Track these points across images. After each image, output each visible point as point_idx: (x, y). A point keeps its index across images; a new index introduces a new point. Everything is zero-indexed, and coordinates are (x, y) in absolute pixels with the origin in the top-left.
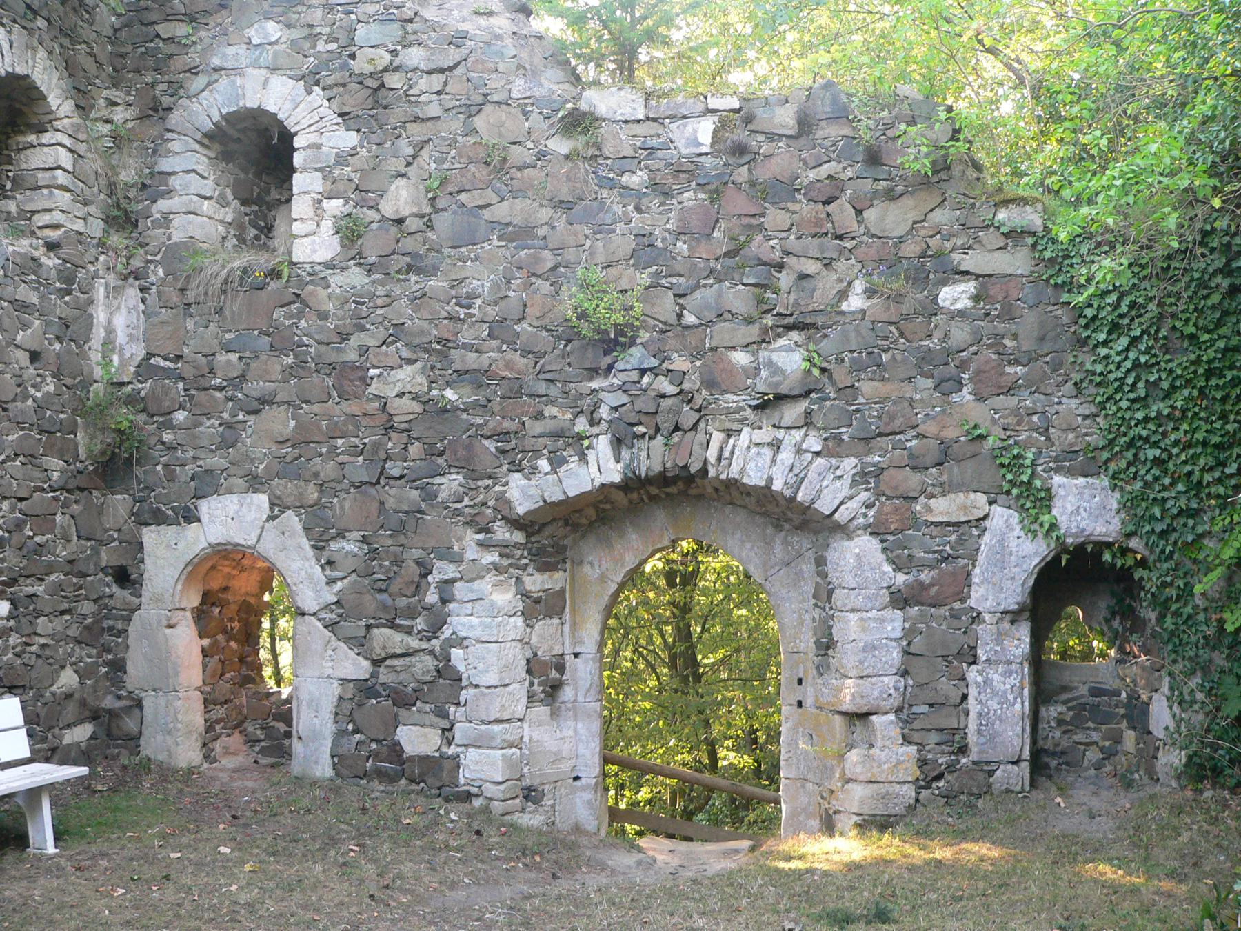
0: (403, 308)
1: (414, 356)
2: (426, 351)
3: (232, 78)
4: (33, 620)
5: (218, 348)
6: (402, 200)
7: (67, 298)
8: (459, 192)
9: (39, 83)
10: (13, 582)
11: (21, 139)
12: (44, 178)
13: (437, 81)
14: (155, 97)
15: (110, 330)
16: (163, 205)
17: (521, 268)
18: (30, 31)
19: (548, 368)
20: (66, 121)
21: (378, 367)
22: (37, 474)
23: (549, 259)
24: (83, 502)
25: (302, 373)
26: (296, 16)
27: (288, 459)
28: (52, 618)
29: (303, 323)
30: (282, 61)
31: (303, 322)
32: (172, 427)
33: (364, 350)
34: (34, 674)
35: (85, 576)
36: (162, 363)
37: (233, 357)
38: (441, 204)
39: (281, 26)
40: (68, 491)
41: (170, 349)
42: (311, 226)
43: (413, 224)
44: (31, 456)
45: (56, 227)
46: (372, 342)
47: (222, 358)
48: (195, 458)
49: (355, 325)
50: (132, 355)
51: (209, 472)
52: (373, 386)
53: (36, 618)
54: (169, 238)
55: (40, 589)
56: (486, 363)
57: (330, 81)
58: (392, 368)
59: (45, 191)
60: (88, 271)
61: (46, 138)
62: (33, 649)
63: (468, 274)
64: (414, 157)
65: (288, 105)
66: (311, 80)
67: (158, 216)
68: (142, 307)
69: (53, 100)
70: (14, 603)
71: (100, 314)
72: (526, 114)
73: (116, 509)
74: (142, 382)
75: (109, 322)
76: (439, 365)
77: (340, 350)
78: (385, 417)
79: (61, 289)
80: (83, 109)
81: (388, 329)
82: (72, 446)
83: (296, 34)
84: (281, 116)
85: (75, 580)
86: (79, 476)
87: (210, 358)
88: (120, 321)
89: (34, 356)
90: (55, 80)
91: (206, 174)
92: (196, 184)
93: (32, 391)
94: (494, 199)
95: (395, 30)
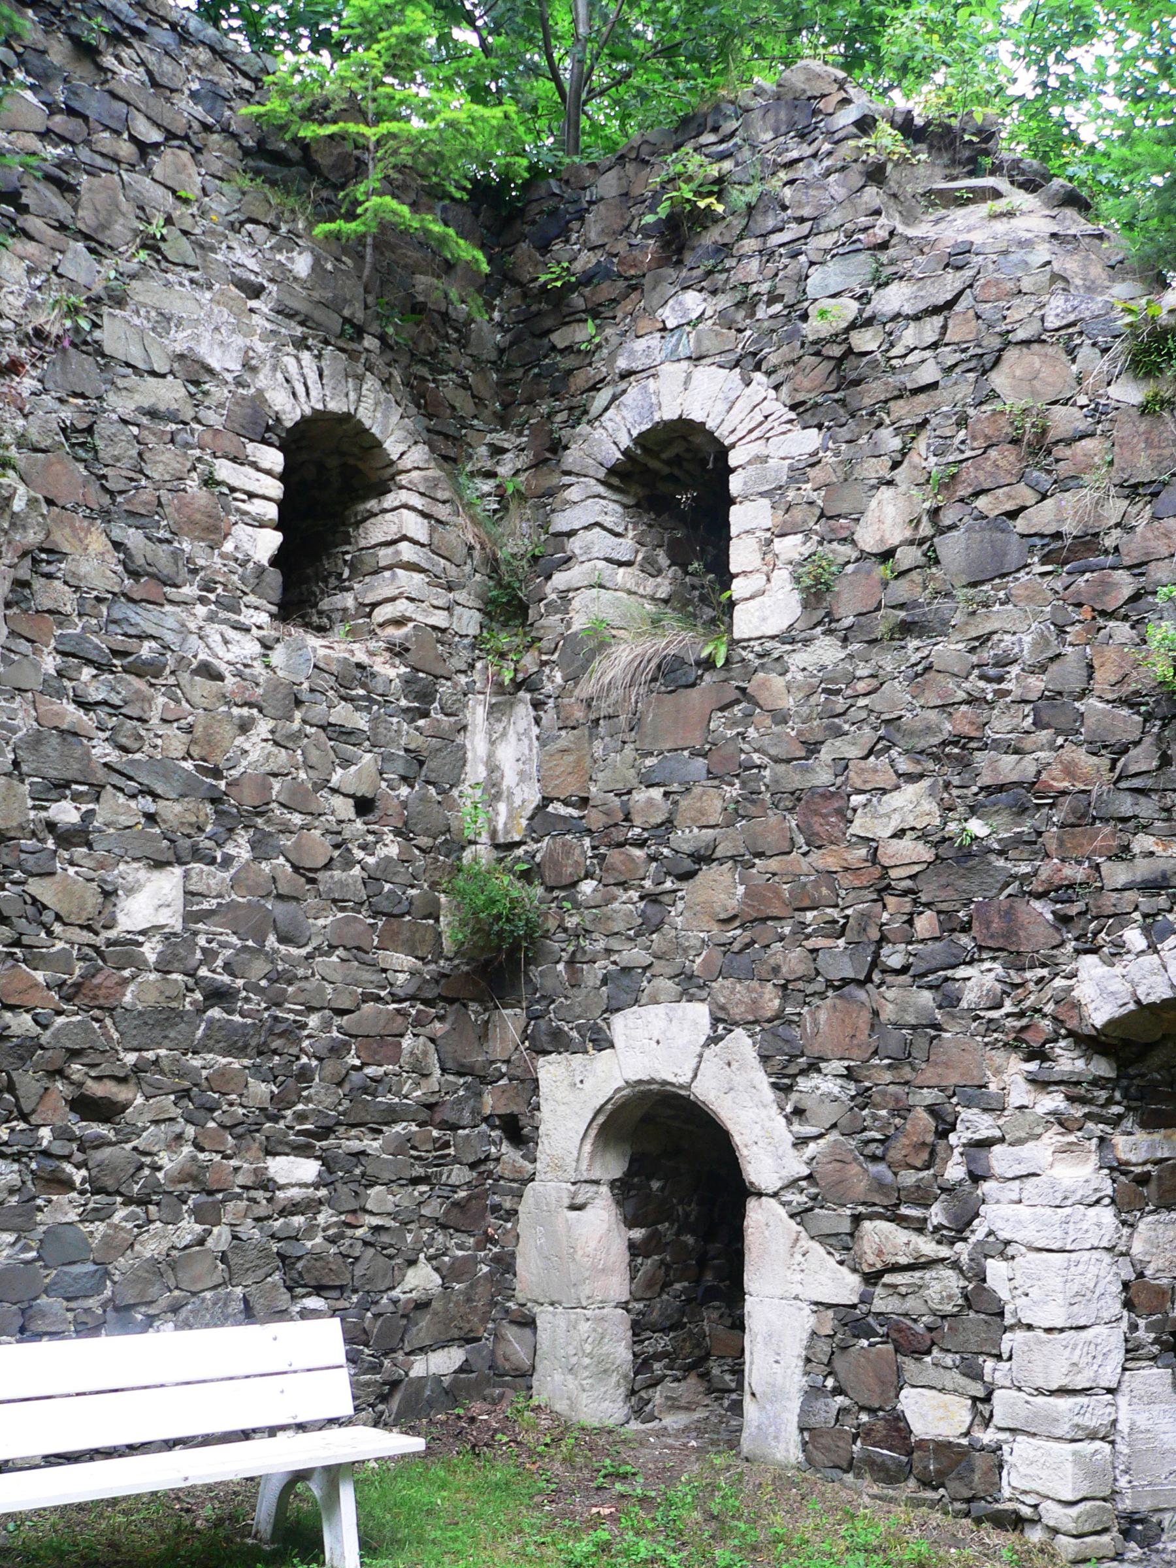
0: (897, 694)
1: (918, 769)
2: (936, 758)
3: (643, 382)
4: (360, 1189)
5: (635, 782)
6: (889, 522)
7: (421, 722)
8: (977, 494)
9: (367, 423)
10: (325, 1132)
11: (361, 507)
12: (386, 555)
13: (930, 329)
14: (551, 432)
15: (493, 768)
16: (560, 579)
17: (1079, 605)
18: (353, 356)
19: (1133, 769)
20: (415, 474)
21: (864, 792)
22: (367, 975)
23: (1125, 584)
24: (450, 1019)
25: (752, 810)
26: (725, 275)
27: (736, 947)
28: (394, 1187)
29: (752, 732)
30: (709, 345)
31: (751, 730)
32: (577, 905)
33: (842, 765)
34: (359, 1270)
35: (454, 1127)
36: (564, 811)
37: (656, 793)
38: (947, 519)
39: (704, 295)
40: (425, 1002)
41: (571, 788)
42: (758, 581)
43: (908, 557)
44: (359, 948)
45: (399, 622)
46: (853, 752)
47: (641, 796)
48: (608, 951)
49: (828, 727)
50: (523, 801)
51: (626, 970)
52: (857, 822)
53: (367, 1187)
54: (568, 627)
55: (373, 1145)
56: (1032, 770)
57: (773, 359)
58: (884, 791)
59: (387, 574)
60: (455, 685)
61: (390, 501)
62: (359, 1232)
63: (995, 625)
64: (904, 452)
65: (722, 406)
66: (749, 362)
67: (554, 596)
68: (536, 731)
69: (393, 447)
70: (328, 1163)
71: (476, 744)
72: (1071, 352)
73: (504, 1028)
74: (537, 841)
75: (491, 756)
76: (956, 781)
77: (807, 770)
78: (877, 872)
79: (407, 710)
80: (454, 460)
81: (876, 729)
82: (429, 937)
83: (724, 301)
84: (710, 425)
85: (435, 1133)
86: (443, 981)
87: (625, 798)
88: (508, 754)
89: (364, 806)
90: (395, 419)
91: (620, 530)
92: (601, 542)
93: (359, 854)
94: (1030, 497)
95: (863, 265)
